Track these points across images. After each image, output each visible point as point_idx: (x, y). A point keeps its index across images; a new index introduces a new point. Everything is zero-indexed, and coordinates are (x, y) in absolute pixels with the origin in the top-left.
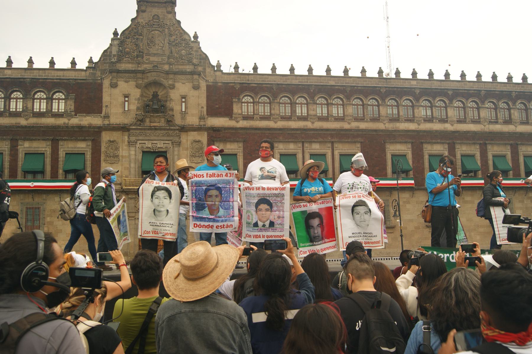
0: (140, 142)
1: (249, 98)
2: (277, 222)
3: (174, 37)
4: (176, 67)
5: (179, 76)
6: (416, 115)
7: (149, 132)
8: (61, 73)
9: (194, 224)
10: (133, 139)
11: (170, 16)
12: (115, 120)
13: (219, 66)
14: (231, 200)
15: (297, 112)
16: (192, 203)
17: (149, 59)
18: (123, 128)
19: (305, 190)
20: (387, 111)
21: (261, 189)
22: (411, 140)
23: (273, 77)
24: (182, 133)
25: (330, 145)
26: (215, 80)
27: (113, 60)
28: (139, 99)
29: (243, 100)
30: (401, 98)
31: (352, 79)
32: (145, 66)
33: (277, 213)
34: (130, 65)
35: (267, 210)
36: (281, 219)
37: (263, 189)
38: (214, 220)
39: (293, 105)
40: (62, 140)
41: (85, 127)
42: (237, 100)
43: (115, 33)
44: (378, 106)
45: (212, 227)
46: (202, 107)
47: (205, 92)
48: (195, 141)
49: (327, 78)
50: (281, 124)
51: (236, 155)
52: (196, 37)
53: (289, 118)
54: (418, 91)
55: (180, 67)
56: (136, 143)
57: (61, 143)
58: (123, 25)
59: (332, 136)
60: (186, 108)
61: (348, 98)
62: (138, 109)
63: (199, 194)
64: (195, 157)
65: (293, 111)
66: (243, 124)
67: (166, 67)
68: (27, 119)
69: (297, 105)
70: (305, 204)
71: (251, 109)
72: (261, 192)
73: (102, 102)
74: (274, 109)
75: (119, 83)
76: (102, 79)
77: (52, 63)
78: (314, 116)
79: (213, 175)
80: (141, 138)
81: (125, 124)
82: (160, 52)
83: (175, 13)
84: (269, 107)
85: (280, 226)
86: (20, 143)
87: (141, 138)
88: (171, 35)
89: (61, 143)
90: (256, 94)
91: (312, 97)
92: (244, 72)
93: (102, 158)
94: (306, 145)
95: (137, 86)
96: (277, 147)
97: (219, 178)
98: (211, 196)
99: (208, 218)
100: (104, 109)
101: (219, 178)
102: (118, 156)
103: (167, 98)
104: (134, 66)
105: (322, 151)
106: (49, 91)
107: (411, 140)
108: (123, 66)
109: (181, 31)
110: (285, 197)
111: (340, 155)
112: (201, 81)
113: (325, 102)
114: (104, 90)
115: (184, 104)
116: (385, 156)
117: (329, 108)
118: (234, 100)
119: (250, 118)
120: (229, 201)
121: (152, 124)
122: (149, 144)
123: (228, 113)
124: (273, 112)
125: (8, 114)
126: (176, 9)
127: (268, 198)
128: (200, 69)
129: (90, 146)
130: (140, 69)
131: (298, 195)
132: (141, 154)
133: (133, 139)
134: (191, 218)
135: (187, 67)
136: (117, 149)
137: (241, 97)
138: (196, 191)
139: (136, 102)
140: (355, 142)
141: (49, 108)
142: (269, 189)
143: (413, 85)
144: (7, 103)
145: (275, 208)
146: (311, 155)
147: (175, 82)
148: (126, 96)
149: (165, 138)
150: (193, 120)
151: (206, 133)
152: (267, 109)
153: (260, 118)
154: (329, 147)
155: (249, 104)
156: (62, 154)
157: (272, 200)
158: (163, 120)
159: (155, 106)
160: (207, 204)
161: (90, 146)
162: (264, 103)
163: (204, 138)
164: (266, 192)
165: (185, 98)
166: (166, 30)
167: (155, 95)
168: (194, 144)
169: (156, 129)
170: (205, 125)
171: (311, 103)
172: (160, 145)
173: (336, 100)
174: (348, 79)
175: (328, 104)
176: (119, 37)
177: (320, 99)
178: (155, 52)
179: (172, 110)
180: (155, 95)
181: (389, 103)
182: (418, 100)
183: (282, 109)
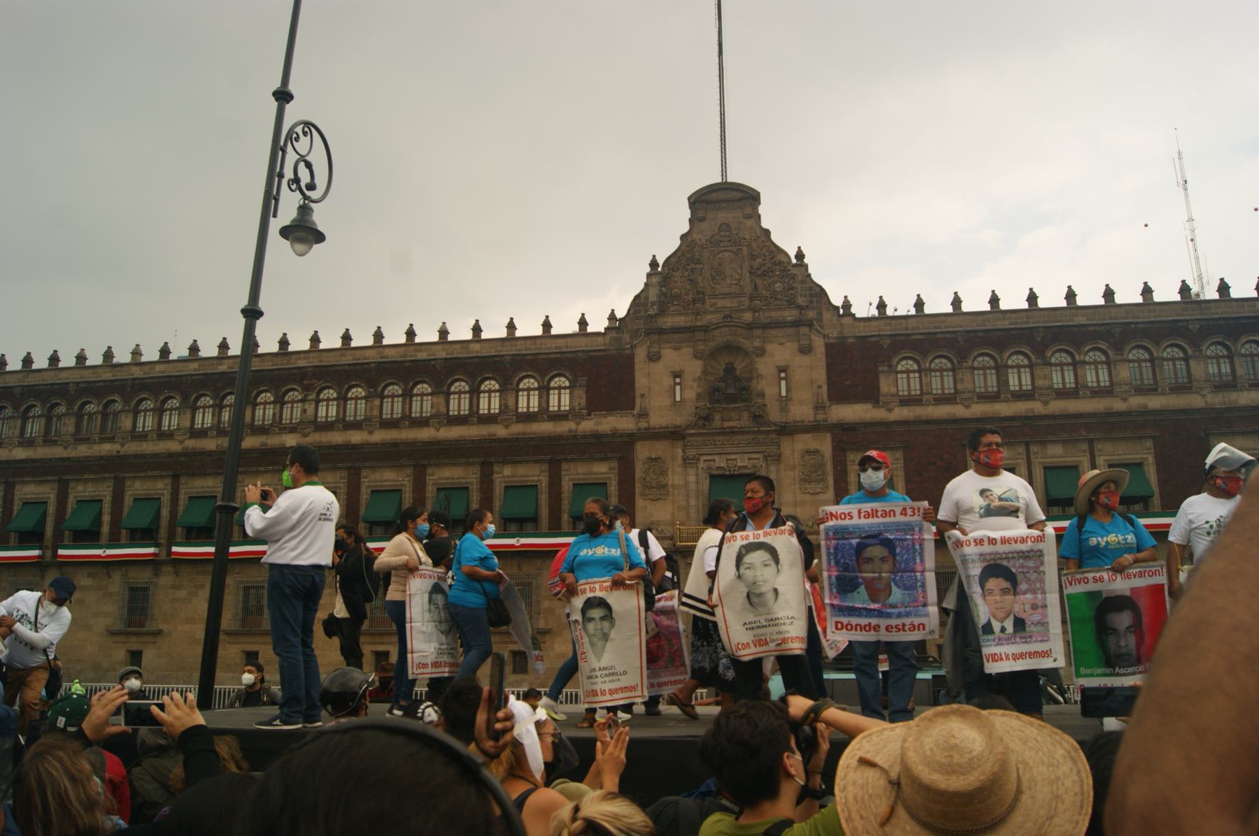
0: (705, 458)
1: (911, 362)
2: (1032, 617)
3: (759, 260)
4: (766, 314)
5: (774, 332)
7: (720, 438)
9: (837, 623)
10: (691, 452)
11: (750, 223)
12: (659, 419)
13: (847, 305)
14: (919, 568)
15: (1011, 383)
16: (830, 577)
17: (715, 304)
18: (673, 435)
19: (1093, 541)
20: (1210, 366)
21: (986, 543)
25: (1085, 446)
27: (651, 312)
28: (699, 379)
29: (899, 368)
30: (1236, 340)
31: (1123, 310)
32: (709, 317)
33: (1029, 596)
34: (682, 318)
35: (1004, 592)
36: (1040, 610)
37: (992, 541)
38: (880, 614)
39: (1001, 370)
40: (566, 460)
41: (606, 435)
43: (654, 264)
44: (1186, 359)
45: (876, 628)
46: (820, 387)
47: (824, 357)
48: (808, 452)
49: (1068, 312)
52: (800, 255)
55: (774, 314)
57: (565, 466)
60: (788, 390)
61: (1118, 347)
62: (699, 396)
63: (843, 556)
64: (810, 482)
65: (1003, 382)
66: (900, 413)
67: (748, 317)
68: (507, 427)
70: (1098, 575)
72: (987, 548)
74: (962, 380)
75: (664, 352)
77: (547, 325)
79: (874, 513)
80: (705, 451)
81: (676, 427)
83: (759, 216)
85: (1039, 628)
86: (496, 468)
87: (705, 451)
88: (753, 257)
90: (924, 353)
92: (897, 314)
93: (638, 489)
94: (1034, 449)
95: (696, 356)
97: (887, 520)
98: (870, 560)
99: (865, 609)
100: (638, 401)
101: (887, 520)
102: (666, 485)
105: (1070, 460)
106: (543, 375)
108: (669, 321)
110: (1046, 559)
113: (1069, 360)
114: (637, 367)
115: (783, 383)
120: (914, 571)
121: (726, 424)
122: (721, 462)
123: (871, 395)
124: (959, 387)
126: (761, 209)
127: (1005, 563)
128: (811, 314)
130: (699, 323)
131: (1077, 556)
133: (691, 452)
134: (828, 609)
135: (787, 313)
136: (664, 473)
137: (894, 362)
138: (836, 548)
139: (696, 385)
140: (1140, 438)
141: (544, 404)
142: (1005, 541)
144: (475, 400)
145: (1023, 586)
146: (1045, 468)
148: (677, 375)
150: (802, 411)
151: (828, 436)
155: (911, 375)
156: (567, 485)
157: (1014, 566)
158: (745, 415)
159: (730, 390)
160: (863, 578)
162: (941, 370)
163: (825, 445)
164: (1000, 548)
165: (784, 371)
166: (745, 249)
167: (730, 370)
168: (807, 458)
170: (825, 420)
171: (1037, 365)
172: (742, 462)
173: (1091, 354)
175: (1075, 364)
177: (1057, 355)
178: (726, 290)
179: (762, 395)
180: (730, 370)
181: (1209, 353)
183: (979, 381)
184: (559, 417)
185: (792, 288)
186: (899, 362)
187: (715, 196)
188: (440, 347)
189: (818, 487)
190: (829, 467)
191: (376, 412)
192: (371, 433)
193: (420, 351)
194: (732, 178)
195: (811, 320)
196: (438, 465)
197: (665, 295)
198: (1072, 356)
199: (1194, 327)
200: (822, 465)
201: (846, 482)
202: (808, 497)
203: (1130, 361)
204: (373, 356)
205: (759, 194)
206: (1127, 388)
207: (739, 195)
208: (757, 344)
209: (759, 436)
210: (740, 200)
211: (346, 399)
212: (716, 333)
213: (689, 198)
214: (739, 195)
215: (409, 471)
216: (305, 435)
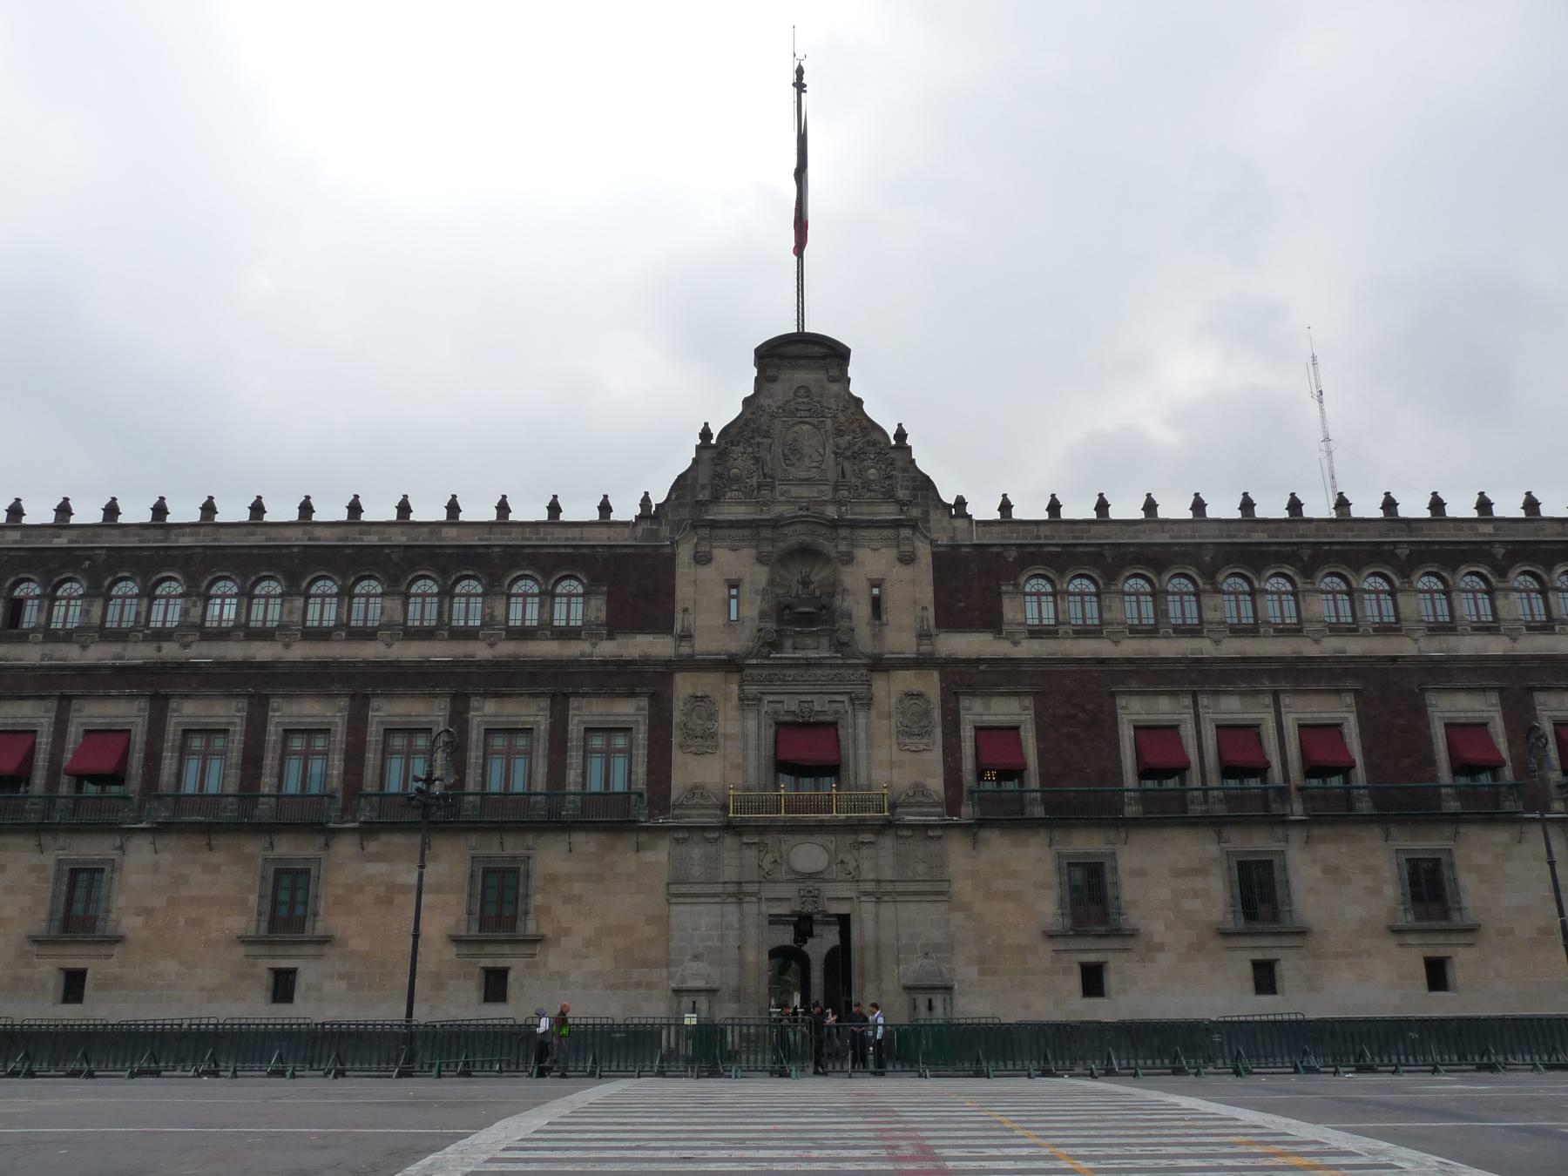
0: (771, 698)
5: (865, 533)
6: (1503, 614)
7: (792, 672)
8: (575, 532)
11: (835, 387)
12: (710, 641)
13: (961, 502)
15: (1172, 614)
18: (730, 665)
22: (1492, 684)
24: (875, 675)
25: (1268, 700)
26: (952, 538)
27: (701, 497)
29: (1028, 589)
31: (1312, 526)
40: (577, 695)
42: (1011, 588)
43: (706, 434)
44: (1392, 593)
46: (924, 608)
48: (910, 695)
49: (1245, 526)
50: (1130, 648)
51: (1016, 728)
52: (901, 435)
53: (1151, 632)
54: (1500, 551)
56: (760, 700)
58: (724, 412)
59: (1273, 675)
61: (1308, 572)
62: (763, 615)
65: (1161, 613)
66: (1029, 649)
67: (831, 512)
68: (492, 645)
69: (1170, 598)
75: (715, 552)
76: (674, 543)
82: (814, 474)
84: (1095, 605)
86: (474, 702)
88: (839, 433)
90: (1061, 571)
91: (1210, 575)
93: (676, 738)
94: (1204, 701)
95: (761, 560)
96: (1126, 708)
100: (679, 616)
103: (834, 588)
104: (751, 509)
105: (1249, 717)
106: (547, 576)
107: (1497, 684)
109: (865, 423)
111: (1300, 726)
112: (918, 544)
114: (679, 571)
116: (1428, 727)
117: (1259, 603)
119: (1049, 632)
122: (792, 704)
123: (992, 622)
125: (446, 634)
128: (915, 512)
129: (642, 709)
132: (772, 731)
133: (752, 690)
135: (884, 509)
136: (712, 716)
137: (1022, 579)
139: (759, 598)
140: (1338, 692)
141: (546, 617)
143: (1484, 535)
147: (853, 546)
148: (733, 584)
149: (833, 689)
150: (900, 639)
151: (936, 675)
152: (1092, 609)
153: (1075, 632)
154: (1267, 706)
156: (575, 729)
158: (825, 642)
161: (642, 709)
163: (930, 684)
166: (829, 422)
168: (908, 702)
169: (809, 665)
170: (932, 653)
171: (1205, 592)
173: (1273, 580)
174: (1302, 526)
175: (1253, 593)
176: (713, 442)
178: (803, 475)
179: (849, 616)
181: (1420, 585)
182: (1502, 573)
184: (567, 634)
185: (890, 477)
188: (398, 530)
190: (937, 715)
191: (297, 617)
192: (287, 646)
193: (369, 534)
195: (915, 520)
196: (386, 696)
197: (720, 476)
198: (1250, 583)
200: (927, 714)
202: (907, 755)
203: (1322, 592)
204: (297, 538)
205: (849, 351)
206: (1320, 626)
207: (823, 351)
208: (843, 548)
209: (843, 671)
210: (824, 357)
211: (251, 597)
212: (787, 531)
213: (757, 351)
214: (823, 351)
215: (343, 702)
216: (185, 646)
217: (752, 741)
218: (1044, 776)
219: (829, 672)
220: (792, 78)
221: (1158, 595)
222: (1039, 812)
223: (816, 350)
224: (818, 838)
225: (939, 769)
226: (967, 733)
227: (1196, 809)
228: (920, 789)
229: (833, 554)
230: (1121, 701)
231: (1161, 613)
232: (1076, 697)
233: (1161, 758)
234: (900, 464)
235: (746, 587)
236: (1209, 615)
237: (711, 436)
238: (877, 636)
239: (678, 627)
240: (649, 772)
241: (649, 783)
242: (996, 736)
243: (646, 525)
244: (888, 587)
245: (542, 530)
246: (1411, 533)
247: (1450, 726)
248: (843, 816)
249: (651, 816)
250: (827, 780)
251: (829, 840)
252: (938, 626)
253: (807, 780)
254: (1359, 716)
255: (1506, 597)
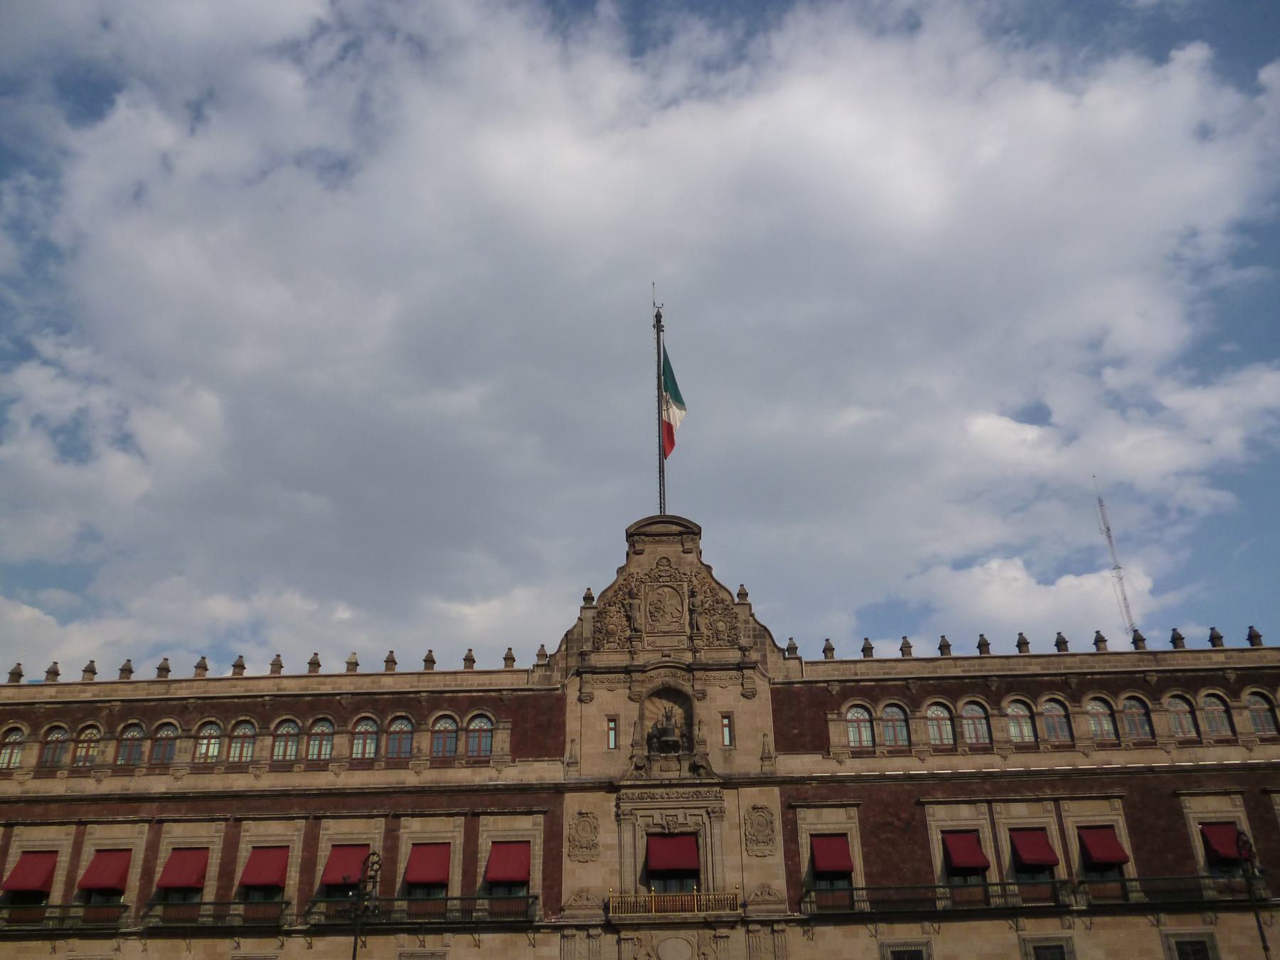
7: (659, 791)
11: (691, 557)
12: (592, 769)
13: (792, 649)
15: (967, 734)
18: (611, 787)
23: (907, 665)
26: (786, 677)
27: (585, 648)
29: (849, 716)
30: (1195, 693)
43: (588, 598)
49: (1022, 660)
51: (845, 835)
52: (743, 594)
53: (952, 751)
54: (1232, 676)
58: (601, 581)
60: (732, 738)
65: (957, 735)
66: (851, 768)
67: (688, 658)
68: (418, 773)
69: (965, 722)
71: (866, 735)
73: (564, 733)
74: (916, 732)
75: (596, 693)
76: (564, 686)
78: (1006, 742)
82: (674, 627)
89: (484, 820)
90: (875, 701)
93: (565, 851)
94: (997, 807)
100: (568, 746)
107: (1237, 788)
109: (714, 585)
116: (1185, 825)
118: (829, 716)
119: (868, 752)
123: (821, 745)
128: (754, 656)
130: (636, 663)
137: (844, 709)
143: (1216, 663)
146: (1011, 830)
150: (747, 763)
154: (1048, 811)
156: (485, 845)
158: (686, 765)
163: (771, 798)
166: (685, 584)
168: (755, 815)
172: (685, 819)
174: (1068, 660)
178: (665, 629)
179: (704, 742)
183: (933, 731)
186: (848, 710)
187: (654, 528)
188: (348, 680)
189: (766, 849)
190: (778, 824)
191: (266, 754)
193: (324, 684)
194: (670, 511)
195: (756, 663)
199: (1153, 678)
201: (797, 843)
202: (755, 861)
206: (1088, 743)
208: (697, 687)
210: (680, 534)
214: (680, 529)
216: (177, 779)
217: (628, 850)
218: (868, 875)
219: (689, 789)
220: (653, 321)
221: (954, 719)
222: (866, 907)
223: (675, 528)
224: (682, 933)
225: (782, 872)
226: (804, 841)
227: (996, 902)
228: (766, 889)
229: (690, 691)
230: (930, 809)
231: (957, 735)
232: (894, 809)
233: (964, 863)
234: (742, 617)
235: (622, 722)
236: (997, 735)
237: (593, 599)
238: (727, 759)
239: (567, 757)
240: (544, 879)
241: (544, 888)
242: (830, 842)
243: (540, 672)
244: (734, 720)
245: (459, 677)
246: (1157, 662)
247: (1207, 827)
248: (703, 914)
249: (546, 915)
250: (690, 881)
251: (692, 934)
252: (776, 750)
253: (673, 882)
254: (1127, 820)
255: (1241, 715)
